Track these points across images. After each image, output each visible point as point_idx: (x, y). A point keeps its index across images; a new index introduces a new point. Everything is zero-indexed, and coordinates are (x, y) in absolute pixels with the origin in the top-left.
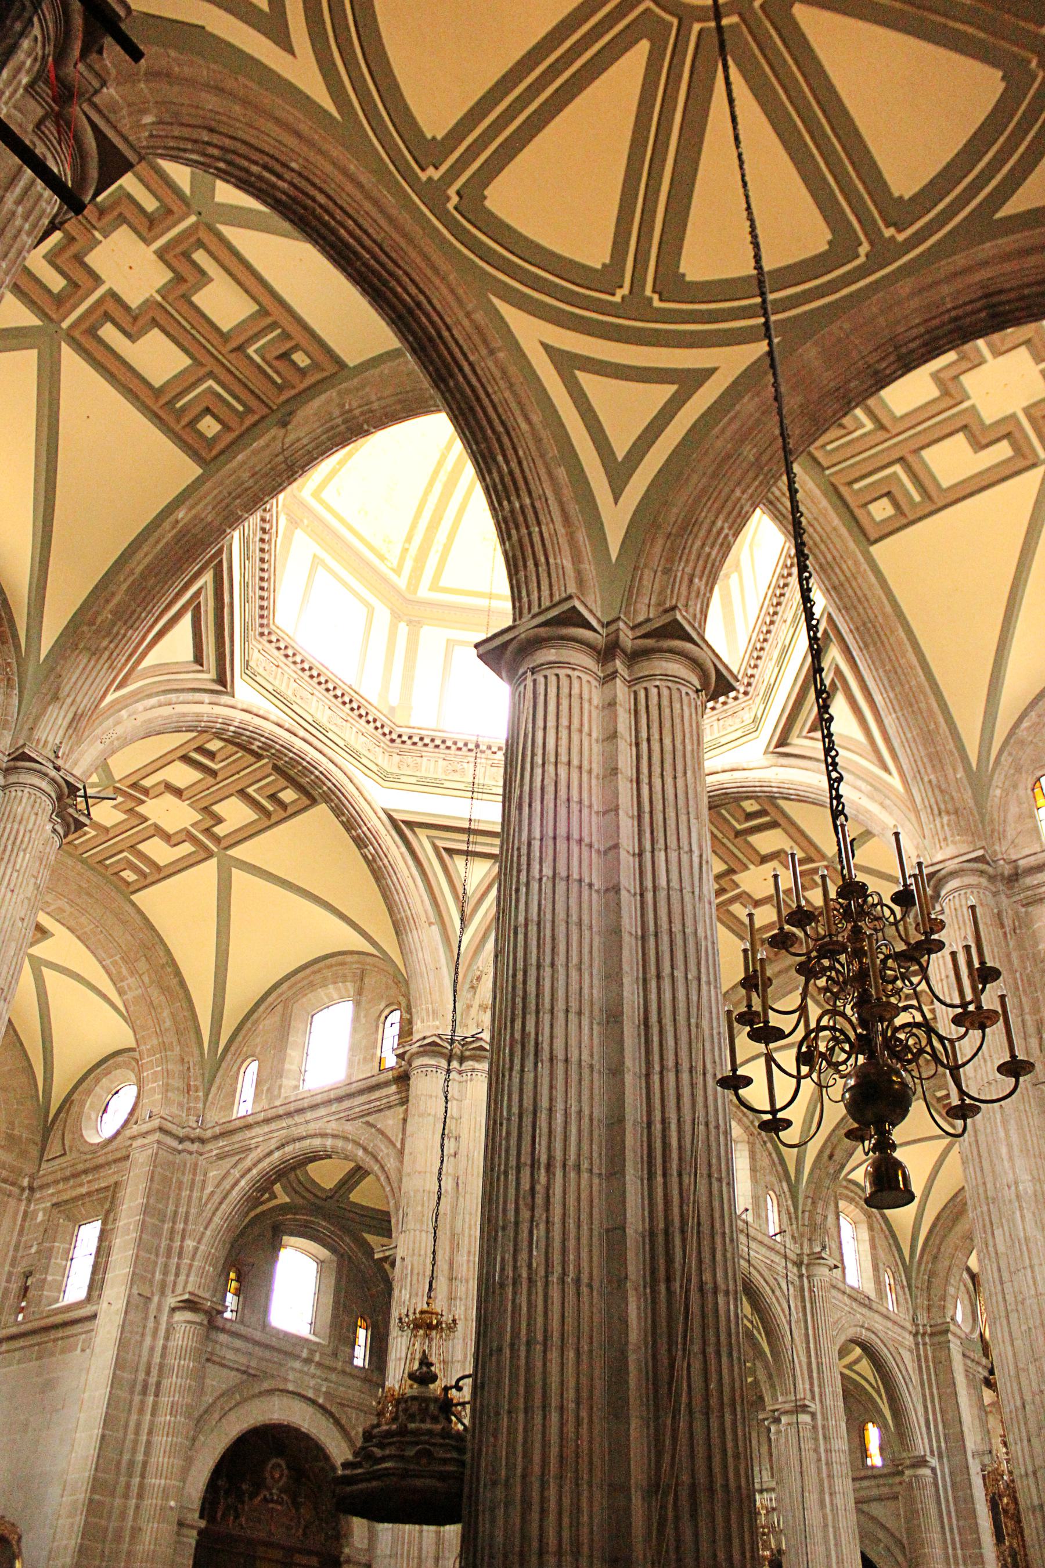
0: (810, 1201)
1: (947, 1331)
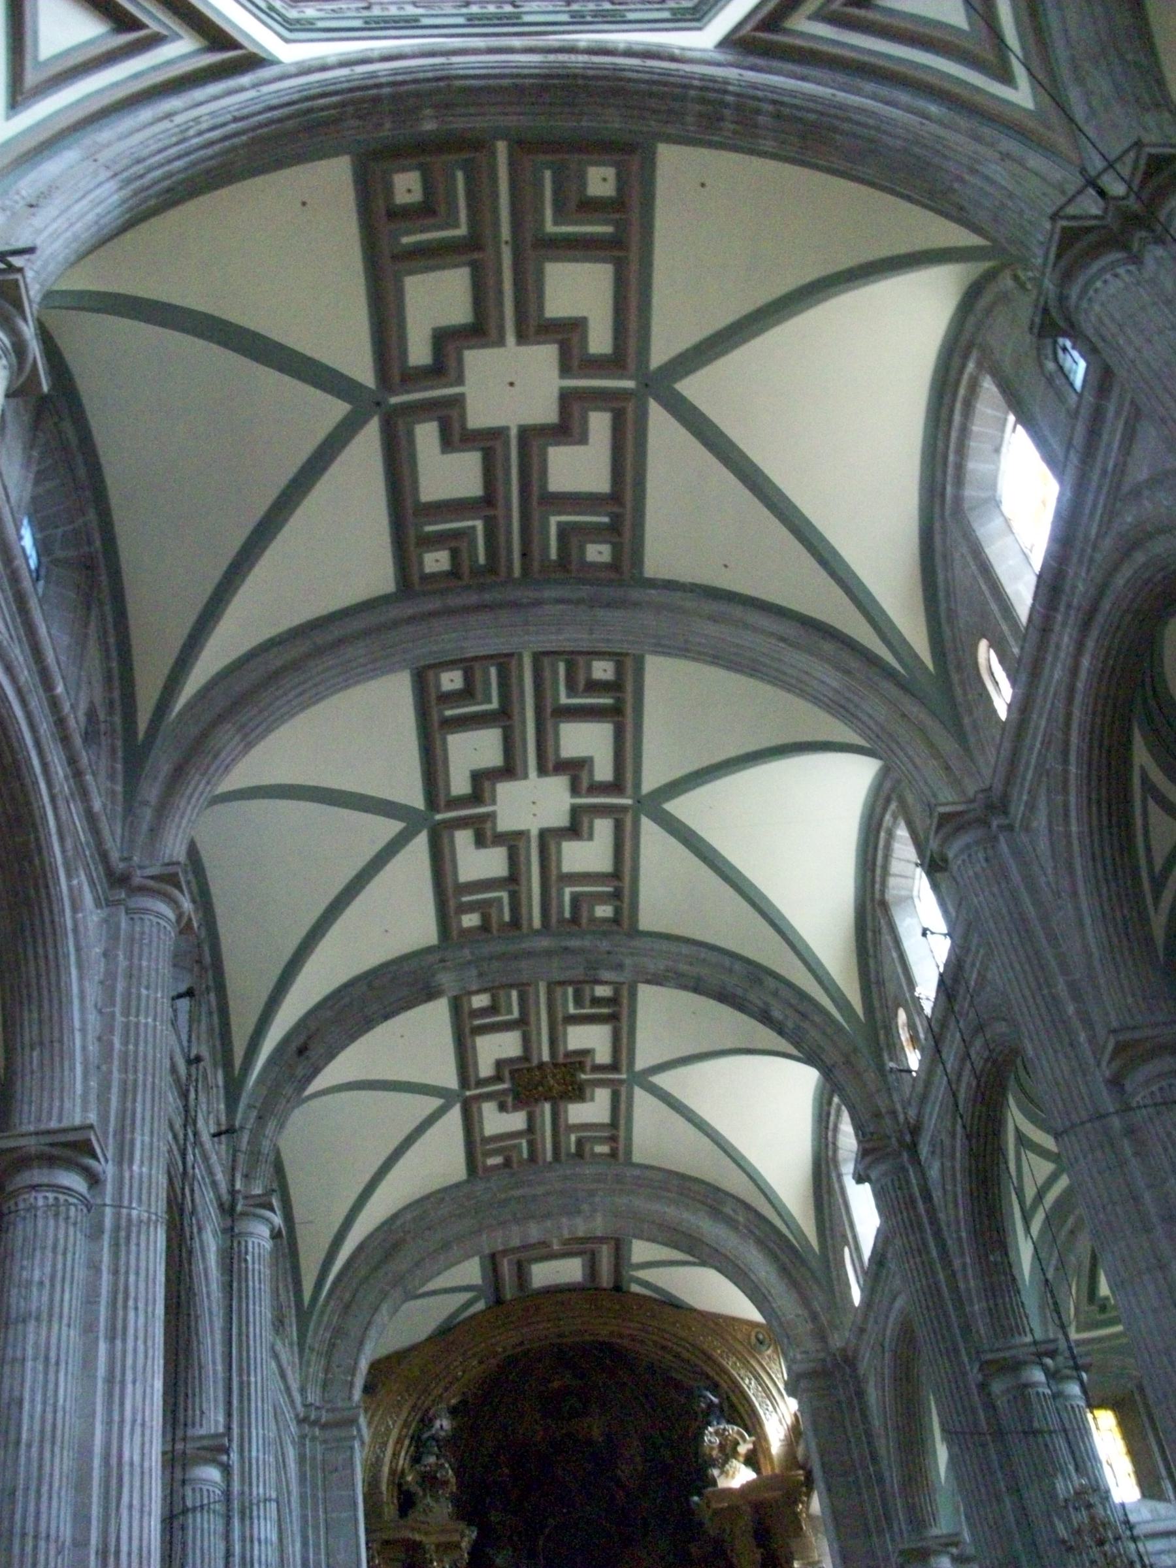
0: (254, 1113)
1: (353, 1421)
